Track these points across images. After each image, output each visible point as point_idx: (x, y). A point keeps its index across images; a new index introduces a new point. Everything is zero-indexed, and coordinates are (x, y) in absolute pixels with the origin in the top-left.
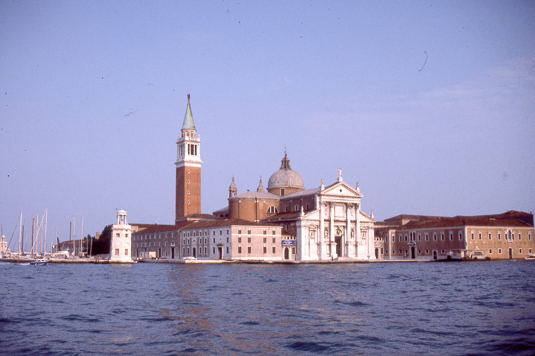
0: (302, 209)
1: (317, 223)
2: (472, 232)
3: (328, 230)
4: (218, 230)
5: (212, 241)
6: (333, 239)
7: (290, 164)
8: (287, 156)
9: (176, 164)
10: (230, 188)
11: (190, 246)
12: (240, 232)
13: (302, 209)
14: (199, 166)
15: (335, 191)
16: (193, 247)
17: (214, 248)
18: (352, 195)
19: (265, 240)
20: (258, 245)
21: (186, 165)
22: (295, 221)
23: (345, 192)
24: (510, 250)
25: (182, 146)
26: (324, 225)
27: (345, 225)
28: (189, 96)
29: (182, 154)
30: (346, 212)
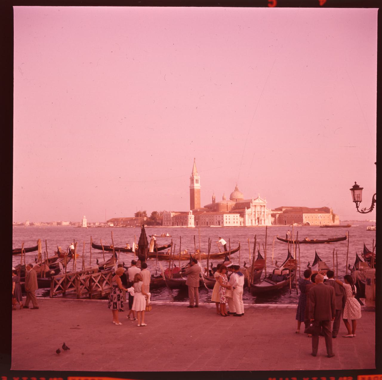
0: (246, 208)
2: (306, 216)
3: (255, 215)
4: (218, 216)
5: (215, 220)
6: (256, 218)
9: (190, 187)
10: (213, 197)
13: (246, 208)
14: (200, 188)
15: (257, 201)
17: (216, 222)
18: (263, 202)
20: (232, 221)
21: (195, 188)
23: (261, 201)
25: (192, 180)
27: (260, 213)
28: (195, 159)
29: (193, 183)
30: (261, 209)
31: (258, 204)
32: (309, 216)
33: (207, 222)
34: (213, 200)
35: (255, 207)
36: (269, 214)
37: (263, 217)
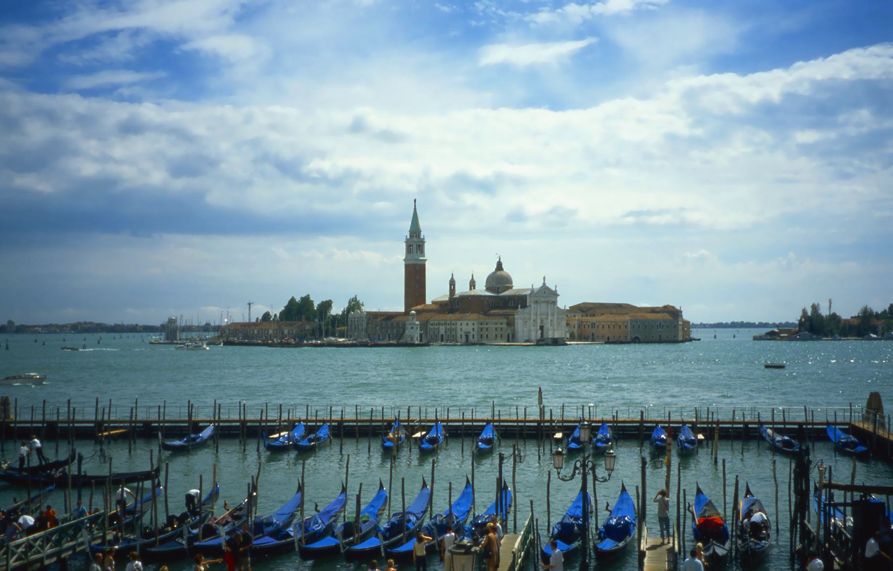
0: (519, 306)
1: (527, 316)
2: (633, 324)
4: (464, 323)
5: (459, 330)
6: (539, 328)
7: (503, 267)
8: (501, 260)
9: (404, 260)
11: (438, 333)
12: (481, 324)
13: (519, 306)
16: (441, 333)
17: (461, 335)
19: (496, 329)
22: (514, 315)
24: (660, 336)
26: (533, 317)
30: (548, 308)
31: (543, 299)
32: (639, 323)
33: (442, 336)
34: (450, 288)
35: (535, 305)
36: (562, 318)
37: (551, 325)
